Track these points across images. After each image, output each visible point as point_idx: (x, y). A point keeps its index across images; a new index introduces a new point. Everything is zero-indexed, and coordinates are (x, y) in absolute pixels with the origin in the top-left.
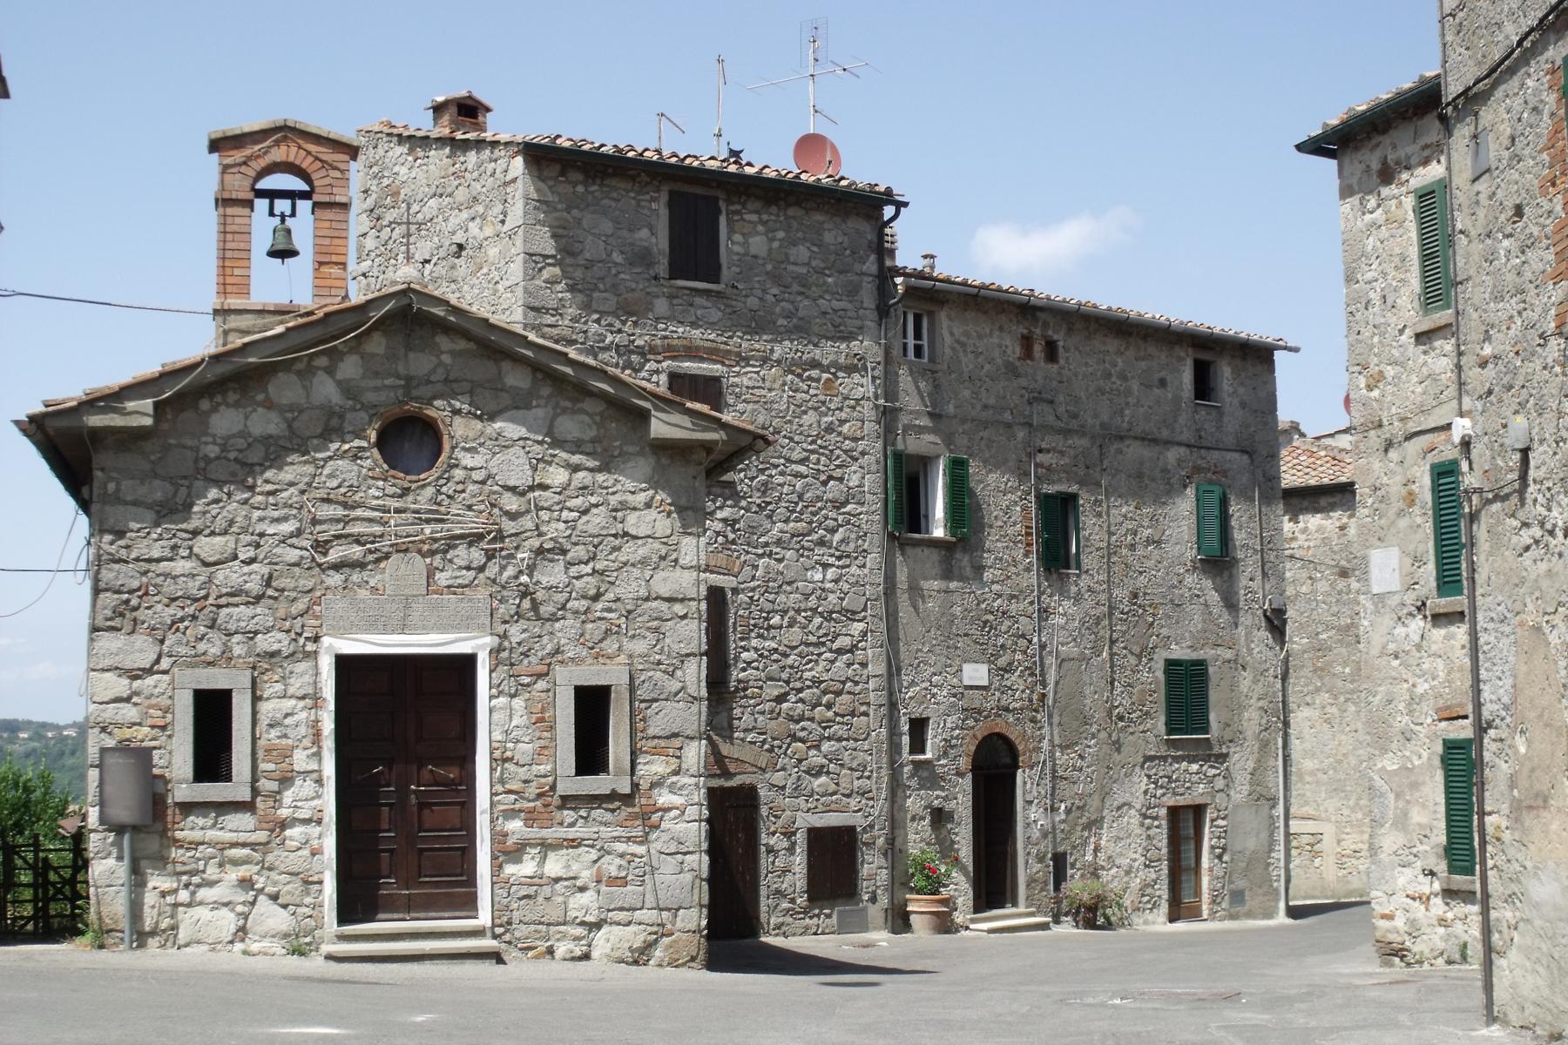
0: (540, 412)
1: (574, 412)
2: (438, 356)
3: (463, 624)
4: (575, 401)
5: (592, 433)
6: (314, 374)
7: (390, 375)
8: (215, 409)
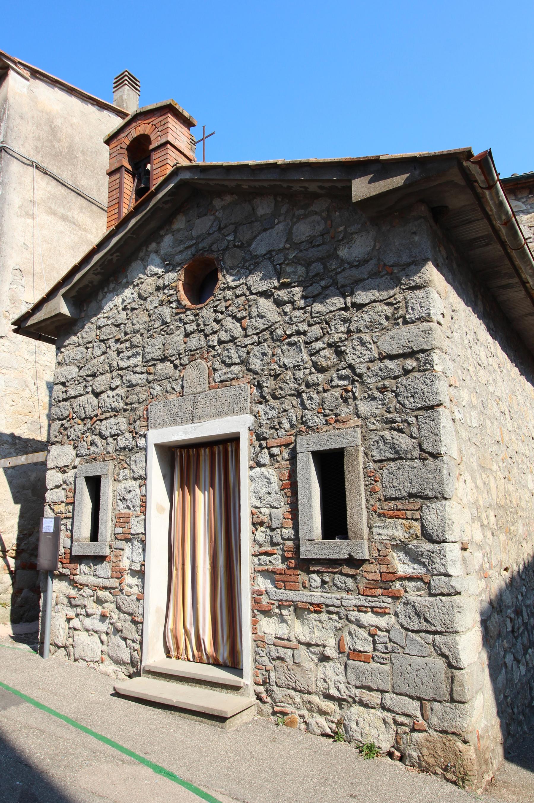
1: (305, 216)
3: (231, 411)
5: (320, 228)
6: (149, 256)
8: (104, 297)
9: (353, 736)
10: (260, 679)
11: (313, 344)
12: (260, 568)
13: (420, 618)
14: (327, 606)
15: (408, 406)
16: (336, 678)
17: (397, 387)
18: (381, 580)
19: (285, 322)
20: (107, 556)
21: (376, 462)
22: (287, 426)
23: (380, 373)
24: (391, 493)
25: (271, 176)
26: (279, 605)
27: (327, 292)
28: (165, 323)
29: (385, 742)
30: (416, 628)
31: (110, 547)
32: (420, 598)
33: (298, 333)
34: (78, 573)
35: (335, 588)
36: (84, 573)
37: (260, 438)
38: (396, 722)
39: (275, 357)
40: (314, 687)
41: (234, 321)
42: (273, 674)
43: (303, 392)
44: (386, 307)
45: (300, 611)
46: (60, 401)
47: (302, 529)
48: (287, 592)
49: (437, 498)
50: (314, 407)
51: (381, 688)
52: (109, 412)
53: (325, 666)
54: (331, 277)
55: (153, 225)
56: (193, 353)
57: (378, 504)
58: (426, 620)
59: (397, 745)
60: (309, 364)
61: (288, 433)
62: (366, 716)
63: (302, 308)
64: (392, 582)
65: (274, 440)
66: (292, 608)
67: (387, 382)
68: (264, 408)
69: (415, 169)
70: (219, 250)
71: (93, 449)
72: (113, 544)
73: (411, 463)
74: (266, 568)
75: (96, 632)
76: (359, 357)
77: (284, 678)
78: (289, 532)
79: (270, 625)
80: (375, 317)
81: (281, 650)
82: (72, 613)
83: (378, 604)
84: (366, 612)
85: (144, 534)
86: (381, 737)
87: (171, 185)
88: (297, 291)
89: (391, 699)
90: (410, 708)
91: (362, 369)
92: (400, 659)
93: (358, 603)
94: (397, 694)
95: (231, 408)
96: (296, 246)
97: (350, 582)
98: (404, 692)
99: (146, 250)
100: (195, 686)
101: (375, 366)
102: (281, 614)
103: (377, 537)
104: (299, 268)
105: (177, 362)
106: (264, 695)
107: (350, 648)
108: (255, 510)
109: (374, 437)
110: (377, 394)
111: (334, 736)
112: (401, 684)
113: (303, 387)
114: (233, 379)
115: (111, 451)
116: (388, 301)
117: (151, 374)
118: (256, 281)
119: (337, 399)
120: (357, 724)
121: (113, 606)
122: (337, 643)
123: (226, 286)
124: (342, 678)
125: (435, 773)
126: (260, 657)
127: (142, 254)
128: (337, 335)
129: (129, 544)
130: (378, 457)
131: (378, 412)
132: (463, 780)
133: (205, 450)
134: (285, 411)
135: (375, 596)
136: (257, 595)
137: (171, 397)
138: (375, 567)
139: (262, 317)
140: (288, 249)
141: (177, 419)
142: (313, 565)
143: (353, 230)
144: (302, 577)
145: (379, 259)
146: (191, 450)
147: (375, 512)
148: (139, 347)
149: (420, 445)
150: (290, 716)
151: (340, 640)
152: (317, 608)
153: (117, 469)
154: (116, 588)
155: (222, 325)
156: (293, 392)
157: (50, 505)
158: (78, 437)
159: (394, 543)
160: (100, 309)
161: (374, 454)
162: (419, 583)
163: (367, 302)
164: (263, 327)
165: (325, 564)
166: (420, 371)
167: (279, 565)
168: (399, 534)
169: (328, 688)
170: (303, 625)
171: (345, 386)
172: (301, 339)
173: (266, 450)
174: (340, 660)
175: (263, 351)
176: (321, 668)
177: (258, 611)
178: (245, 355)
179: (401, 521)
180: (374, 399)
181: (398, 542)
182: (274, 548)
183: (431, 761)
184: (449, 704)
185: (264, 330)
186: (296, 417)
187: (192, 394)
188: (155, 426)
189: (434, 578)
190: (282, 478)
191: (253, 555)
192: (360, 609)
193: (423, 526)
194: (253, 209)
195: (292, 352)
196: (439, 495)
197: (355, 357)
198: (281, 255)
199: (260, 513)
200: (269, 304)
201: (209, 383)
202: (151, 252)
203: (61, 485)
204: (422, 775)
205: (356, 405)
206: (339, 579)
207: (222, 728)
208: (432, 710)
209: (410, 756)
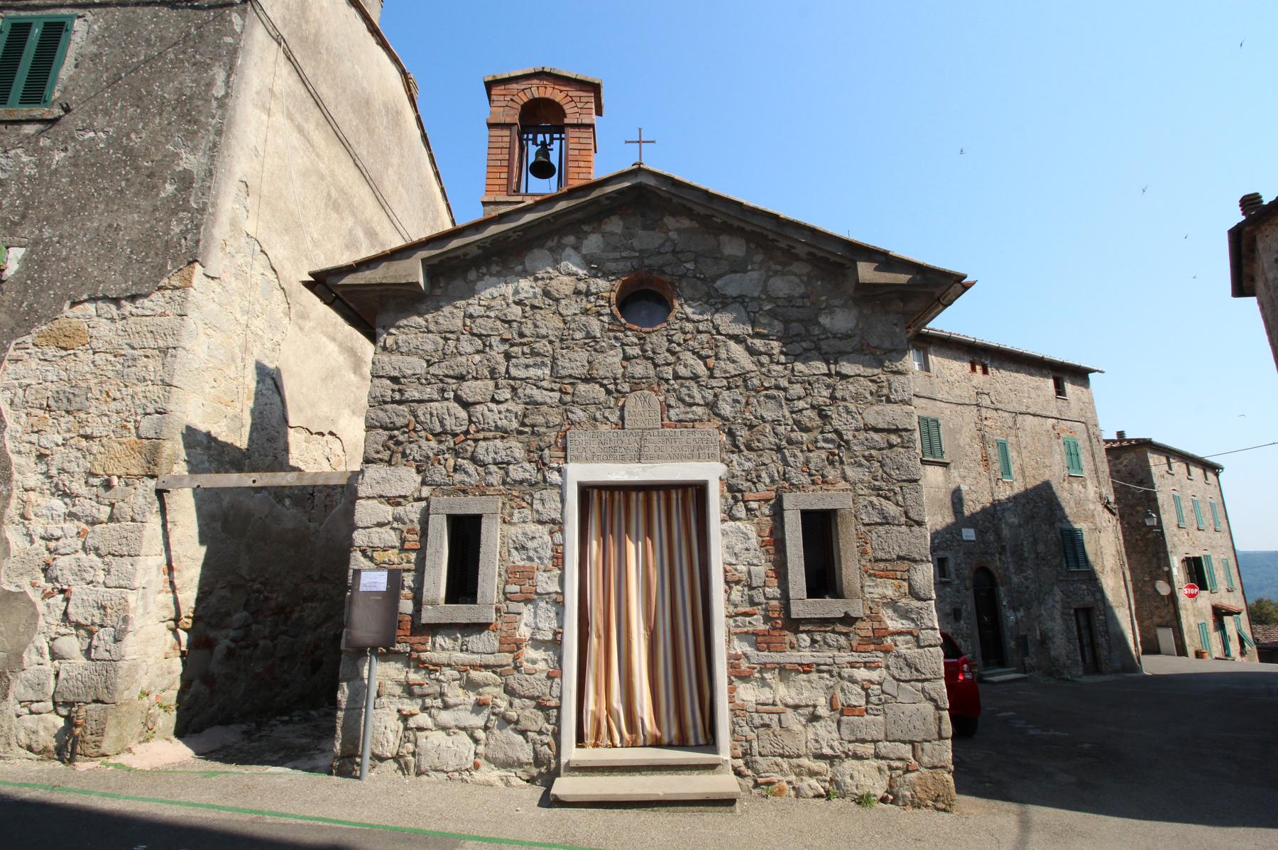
0: (755, 275)
1: (783, 274)
2: (666, 233)
3: (695, 454)
4: (784, 265)
5: (801, 290)
6: (564, 249)
7: (626, 249)
8: (480, 278)
10: (739, 751)
12: (738, 630)
14: (818, 665)
16: (829, 736)
21: (865, 525)
22: (768, 481)
24: (880, 555)
25: (769, 225)
28: (589, 336)
29: (878, 787)
31: (498, 610)
33: (778, 387)
36: (442, 649)
37: (732, 489)
45: (784, 671)
46: (385, 403)
54: (812, 341)
55: (579, 215)
58: (917, 670)
67: (873, 452)
71: (458, 477)
75: (464, 729)
78: (773, 591)
82: (410, 706)
83: (871, 659)
85: (562, 594)
88: (775, 344)
89: (884, 747)
91: (848, 436)
92: (892, 708)
93: (851, 659)
96: (770, 299)
97: (842, 640)
99: (559, 241)
102: (763, 679)
104: (776, 322)
105: (611, 387)
106: (743, 768)
110: (865, 462)
111: (828, 796)
113: (784, 443)
117: (567, 393)
118: (725, 321)
120: (852, 777)
121: (500, 691)
124: (836, 735)
125: (927, 806)
127: (550, 244)
129: (530, 606)
130: (867, 521)
134: (764, 464)
136: (733, 662)
137: (604, 428)
139: (734, 362)
141: (612, 454)
144: (789, 637)
146: (616, 493)
149: (906, 513)
152: (806, 668)
157: (364, 552)
158: (428, 457)
160: (471, 292)
162: (909, 637)
167: (761, 626)
168: (890, 592)
170: (788, 687)
172: (782, 394)
176: (810, 729)
178: (711, 398)
180: (861, 465)
183: (923, 796)
188: (577, 459)
192: (852, 665)
193: (910, 585)
195: (769, 405)
198: (755, 304)
204: (916, 810)
206: (831, 638)
209: (904, 796)
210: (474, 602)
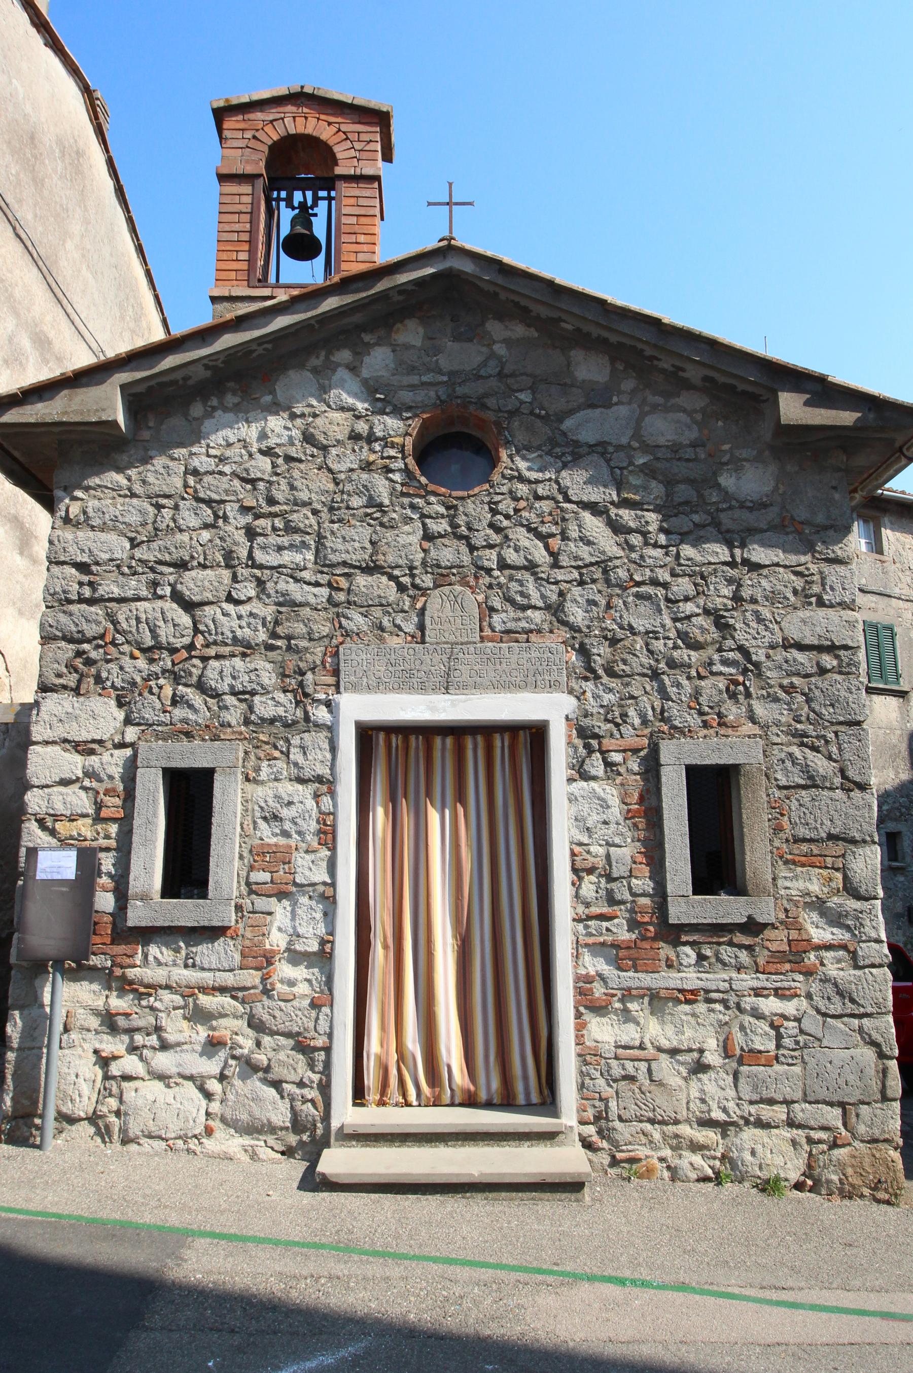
0: (623, 410)
1: (667, 409)
2: (489, 346)
3: (532, 682)
4: (667, 395)
5: (692, 434)
6: (334, 371)
7: (429, 370)
8: (209, 414)
9: (747, 1172)
10: (590, 1114)
11: (681, 604)
12: (591, 940)
13: (844, 998)
14: (707, 991)
15: (827, 717)
16: (721, 1094)
17: (810, 689)
18: (790, 951)
19: (630, 561)
20: (229, 928)
21: (780, 788)
22: (637, 721)
23: (785, 666)
24: (803, 832)
25: (646, 335)
26: (623, 995)
27: (702, 533)
28: (372, 503)
29: (792, 1169)
30: (839, 1011)
31: (239, 908)
32: (841, 973)
33: (655, 582)
34: (138, 963)
35: (720, 966)
36: (157, 964)
37: (584, 733)
38: (810, 1141)
39: (612, 611)
40: (685, 1113)
41: (531, 536)
42: (615, 1103)
43: (663, 673)
44: (793, 578)
45: (657, 1000)
46: (70, 602)
47: (673, 880)
48: (640, 975)
49: (864, 841)
50: (684, 699)
51: (788, 1098)
52: (226, 644)
53: (700, 1080)
54: (709, 513)
55: (357, 318)
56: (444, 571)
57: (784, 846)
58: (853, 1001)
59: (810, 1172)
60: (673, 634)
61: (639, 733)
62: (766, 1140)
63: (662, 547)
64: (805, 952)
65: (613, 741)
66: (646, 999)
67: (796, 680)
68: (593, 687)
69: (870, 410)
70: (500, 410)
71: (179, 713)
72: (247, 903)
73: (831, 793)
74: (601, 939)
75: (191, 1078)
76: (755, 638)
77: (633, 1106)
78: (643, 883)
79: (604, 1028)
80: (778, 587)
81: (629, 1065)
82: (112, 1045)
83: (786, 984)
84: (766, 997)
85: (333, 885)
86: (789, 1165)
87: (430, 270)
88: (652, 517)
89: (802, 1112)
90: (829, 1118)
91: (759, 655)
92: (815, 1056)
93: (756, 984)
94: (810, 1103)
95: (531, 679)
96: (646, 448)
97: (744, 956)
98: (821, 1098)
99: (327, 358)
100: (463, 1146)
101: (779, 655)
102: (626, 1011)
103: (782, 892)
104: (654, 484)
105: (406, 580)
106: (595, 1138)
107: (742, 1049)
108: (577, 849)
109: (777, 753)
110: (782, 695)
111: (718, 1179)
112: (816, 1087)
113: (662, 665)
114: (531, 631)
115: (234, 722)
116: (798, 569)
117: (339, 589)
118: (575, 481)
119: (720, 691)
120: (753, 1153)
121: (242, 1024)
122: (721, 1044)
123: (516, 474)
124: (731, 1093)
125: (862, 1196)
126: (592, 1079)
127: (315, 362)
128: (719, 600)
129: (286, 903)
130: (783, 782)
131: (783, 720)
132: (896, 1195)
133: (417, 738)
134: (632, 697)
135: (781, 974)
137: (394, 642)
138: (781, 934)
139: (589, 543)
140: (635, 449)
141: (406, 681)
142: (687, 933)
143: (744, 456)
144: (666, 951)
145: (783, 507)
146: (413, 738)
147: (781, 857)
148: (309, 534)
149: (842, 771)
150: (644, 1163)
151: (727, 1039)
152: (689, 996)
153: (253, 757)
154: (254, 987)
155: (506, 537)
156: (645, 671)
157: (41, 823)
158: (134, 684)
159: (808, 900)
160: (195, 436)
161: (779, 777)
162: (841, 953)
163: (767, 563)
164: (589, 559)
165: (706, 931)
166: (840, 673)
167: (625, 935)
168: (815, 887)
169: (709, 1111)
170: (663, 1023)
171: (731, 675)
172: (660, 592)
173: (598, 754)
174: (727, 1067)
175: (591, 597)
176: (694, 1086)
177: (586, 1007)
178: (554, 597)
179: (817, 870)
180: (776, 700)
181: (814, 899)
182: (615, 908)
183: (857, 1181)
184: (879, 1105)
185: (592, 564)
186: (653, 708)
187: (447, 643)
188: (355, 688)
189: (863, 945)
190: (628, 800)
191: (574, 920)
192: (758, 992)
193: (846, 878)
194: (569, 365)
195: (642, 609)
196: (868, 838)
197: (749, 637)
198: (622, 454)
199: (588, 852)
200: (600, 525)
201: (481, 630)
202: (338, 365)
203: (78, 779)
204: (846, 1202)
205: (750, 705)
206: (726, 952)
207: (577, 1200)
208: (857, 1115)
209: (829, 1182)
210: (204, 895)
